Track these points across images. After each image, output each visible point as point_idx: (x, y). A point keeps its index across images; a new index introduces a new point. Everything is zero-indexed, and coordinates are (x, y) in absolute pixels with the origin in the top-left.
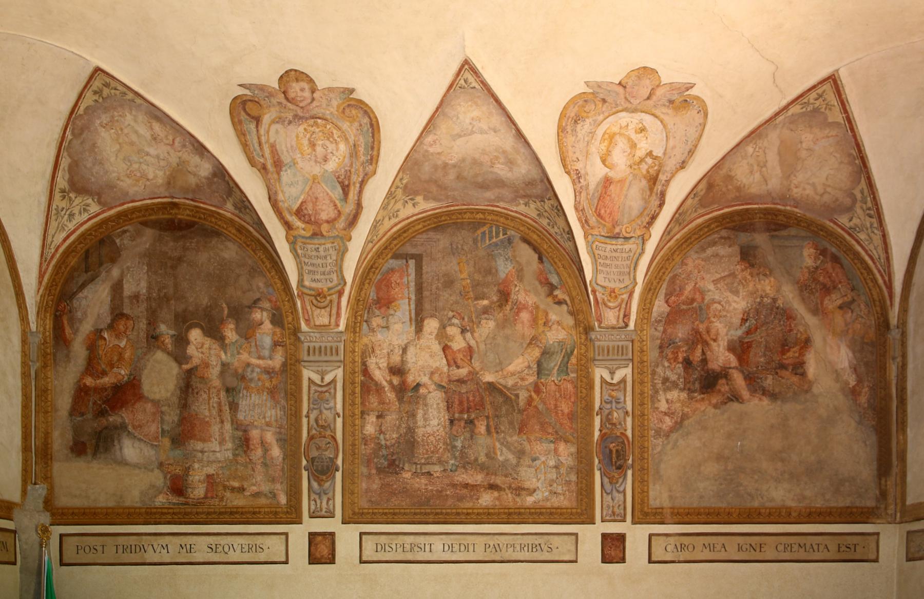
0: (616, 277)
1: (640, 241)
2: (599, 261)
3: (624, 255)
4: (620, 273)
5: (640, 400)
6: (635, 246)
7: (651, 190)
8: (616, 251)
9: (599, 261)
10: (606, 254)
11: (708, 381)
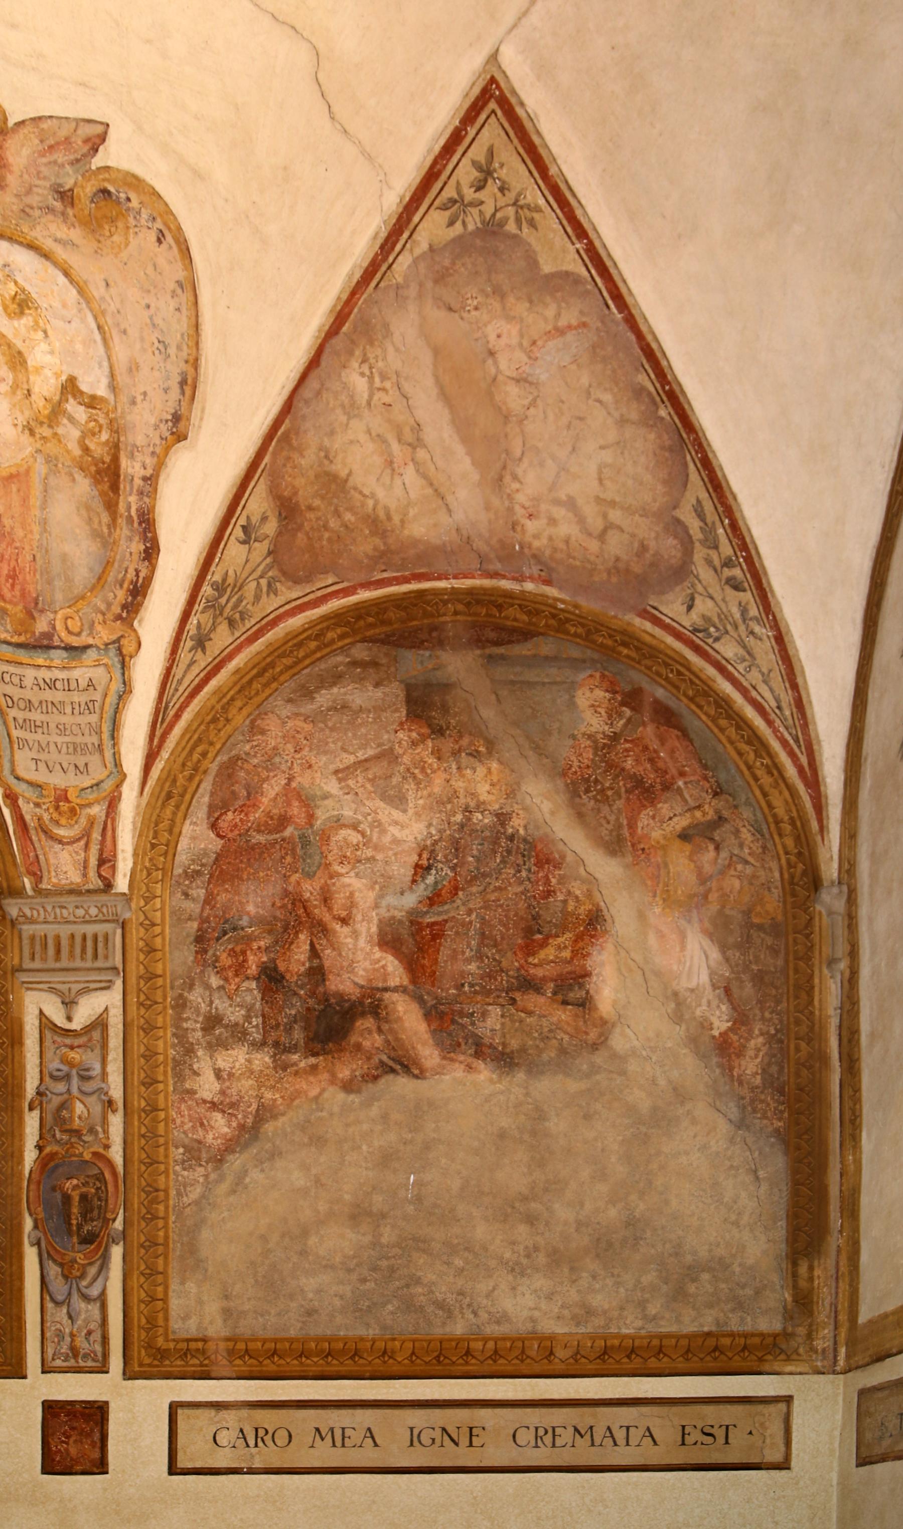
0: (65, 760)
1: (112, 658)
2: (12, 713)
3: (76, 697)
4: (75, 748)
5: (144, 1073)
6: (101, 670)
7: (111, 506)
8: (52, 685)
9: (12, 713)
10: (28, 694)
11: (328, 1024)
